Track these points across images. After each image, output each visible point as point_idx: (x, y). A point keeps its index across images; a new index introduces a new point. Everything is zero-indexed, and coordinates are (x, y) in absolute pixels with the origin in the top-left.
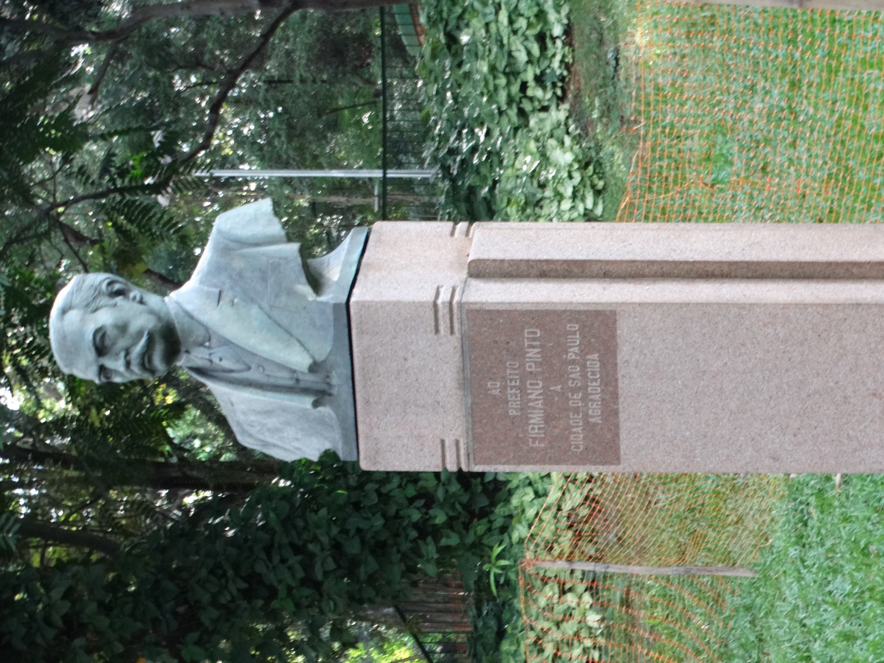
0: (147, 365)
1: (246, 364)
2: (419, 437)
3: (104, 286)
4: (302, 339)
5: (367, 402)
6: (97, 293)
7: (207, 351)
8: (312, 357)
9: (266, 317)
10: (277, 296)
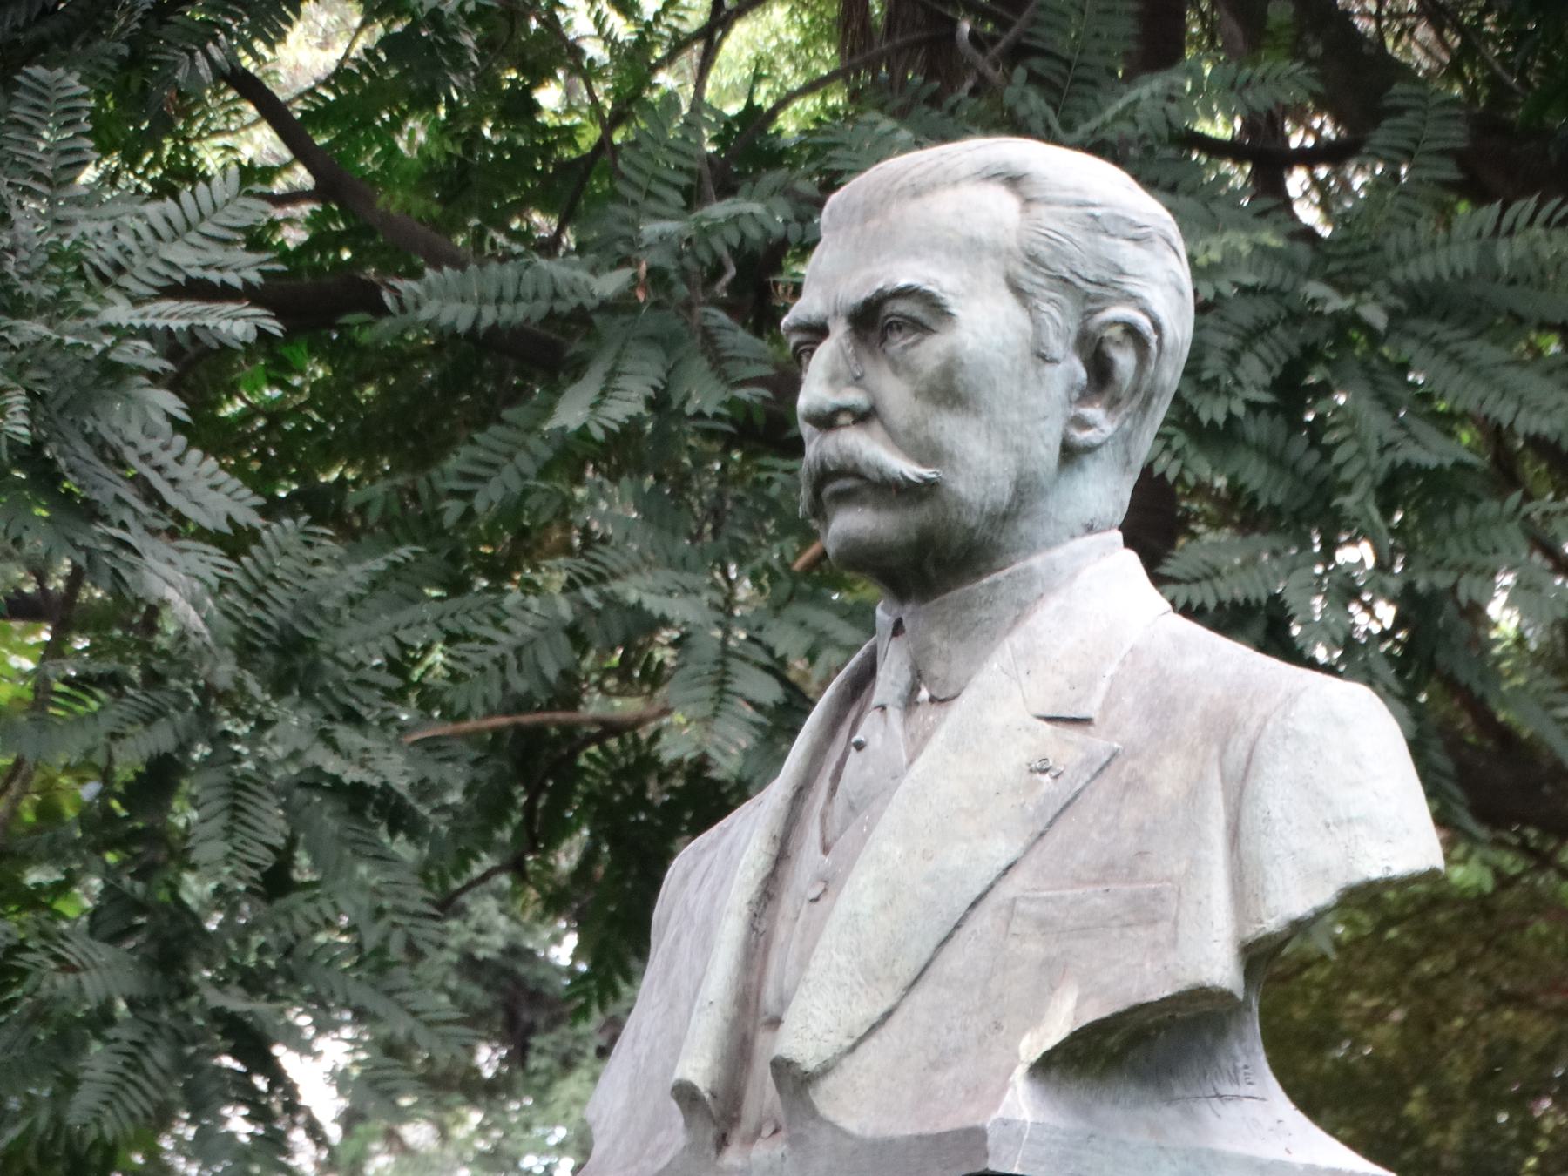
0: (830, 488)
4: (896, 1020)
8: (826, 1070)
10: (1043, 924)
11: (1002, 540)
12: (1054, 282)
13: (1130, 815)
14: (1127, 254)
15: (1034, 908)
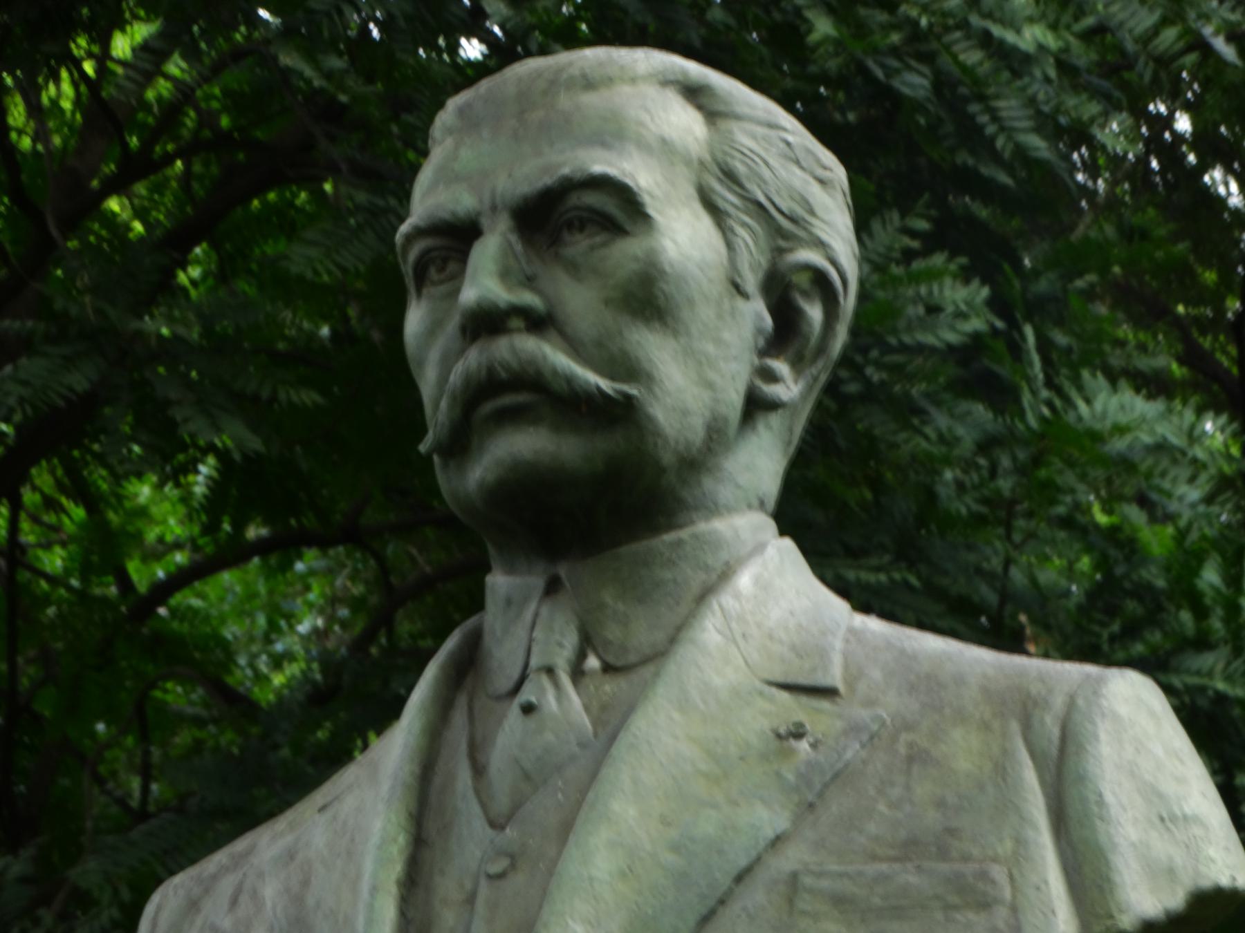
0: (488, 407)
1: (516, 806)
3: (807, 255)
6: (782, 227)
7: (562, 660)
9: (743, 862)
10: (840, 901)
11: (685, 494)
12: (751, 206)
13: (923, 790)
14: (817, 194)
15: (825, 884)
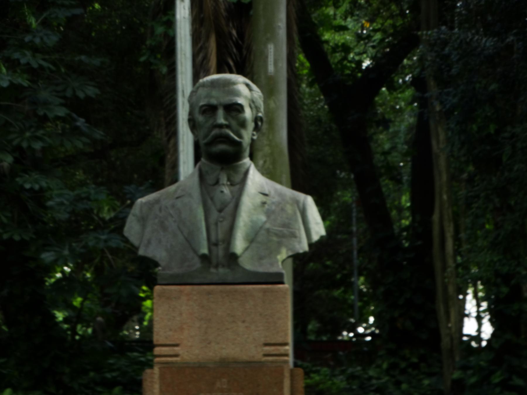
2: (181, 329)
5: (209, 293)
10: (276, 235)
